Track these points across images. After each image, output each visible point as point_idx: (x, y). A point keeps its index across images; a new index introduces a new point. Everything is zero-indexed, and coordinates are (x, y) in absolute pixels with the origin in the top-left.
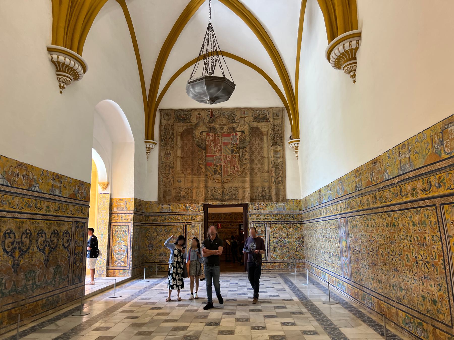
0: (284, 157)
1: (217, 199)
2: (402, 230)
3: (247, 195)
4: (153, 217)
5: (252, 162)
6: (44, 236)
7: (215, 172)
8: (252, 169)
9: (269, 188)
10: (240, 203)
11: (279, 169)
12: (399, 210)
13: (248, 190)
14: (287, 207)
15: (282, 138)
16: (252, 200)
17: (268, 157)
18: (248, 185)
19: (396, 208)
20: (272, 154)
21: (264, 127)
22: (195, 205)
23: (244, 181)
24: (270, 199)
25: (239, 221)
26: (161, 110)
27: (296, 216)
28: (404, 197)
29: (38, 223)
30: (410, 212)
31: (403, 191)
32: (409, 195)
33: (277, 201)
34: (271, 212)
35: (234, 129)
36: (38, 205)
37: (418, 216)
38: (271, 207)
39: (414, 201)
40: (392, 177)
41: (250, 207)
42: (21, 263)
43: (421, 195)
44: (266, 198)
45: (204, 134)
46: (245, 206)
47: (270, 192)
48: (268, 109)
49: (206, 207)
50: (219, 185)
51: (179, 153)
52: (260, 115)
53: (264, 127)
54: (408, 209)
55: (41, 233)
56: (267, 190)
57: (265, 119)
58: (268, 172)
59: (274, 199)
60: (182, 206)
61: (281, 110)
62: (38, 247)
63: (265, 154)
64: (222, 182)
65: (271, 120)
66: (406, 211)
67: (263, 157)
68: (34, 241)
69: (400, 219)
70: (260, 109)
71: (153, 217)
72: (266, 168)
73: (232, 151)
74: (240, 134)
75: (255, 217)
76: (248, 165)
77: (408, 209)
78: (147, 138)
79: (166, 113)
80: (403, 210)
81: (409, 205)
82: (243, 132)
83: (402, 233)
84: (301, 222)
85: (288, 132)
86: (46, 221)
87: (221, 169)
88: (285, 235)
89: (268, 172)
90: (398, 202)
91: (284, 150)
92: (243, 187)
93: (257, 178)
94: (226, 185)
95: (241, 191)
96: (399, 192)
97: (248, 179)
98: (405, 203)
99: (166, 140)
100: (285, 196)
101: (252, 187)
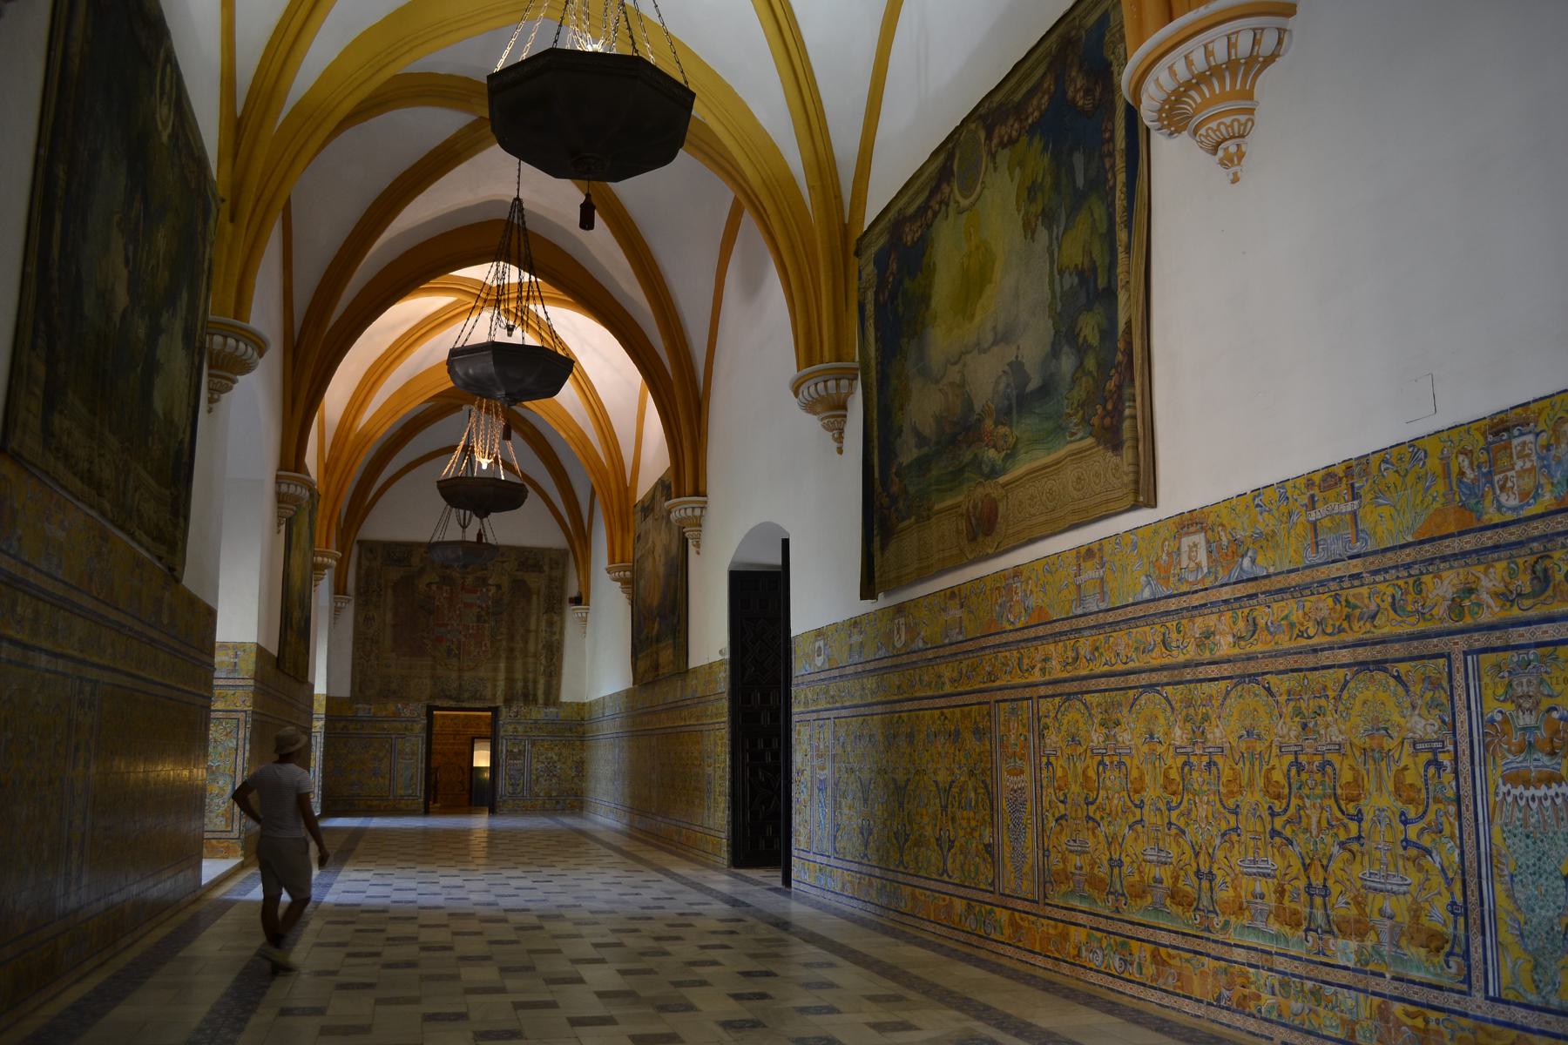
0: (562, 633)
1: (450, 698)
3: (500, 693)
4: (342, 724)
5: (511, 638)
7: (449, 651)
8: (511, 650)
9: (535, 682)
10: (487, 705)
11: (554, 652)
13: (501, 684)
14: (562, 715)
15: (561, 601)
16: (508, 701)
17: (537, 631)
18: (502, 676)
20: (543, 625)
21: (535, 581)
22: (412, 706)
23: (496, 669)
24: (535, 701)
25: (471, 731)
26: (361, 543)
27: (575, 727)
33: (546, 704)
34: (536, 721)
35: (483, 581)
38: (538, 713)
41: (504, 711)
44: (529, 698)
45: (434, 587)
46: (495, 711)
47: (535, 689)
48: (542, 551)
49: (430, 709)
50: (454, 675)
51: (389, 616)
52: (529, 559)
53: (535, 581)
56: (531, 685)
57: (537, 568)
58: (535, 656)
59: (541, 701)
60: (391, 707)
61: (563, 554)
63: (533, 627)
64: (460, 670)
65: (546, 568)
67: (528, 631)
70: (530, 550)
71: (342, 724)
72: (531, 648)
73: (479, 618)
74: (493, 589)
75: (510, 728)
76: (504, 643)
78: (337, 592)
79: (368, 547)
82: (499, 587)
84: (582, 738)
85: (573, 590)
87: (459, 648)
88: (555, 758)
89: (535, 656)
91: (562, 621)
92: (495, 680)
93: (518, 665)
94: (467, 675)
95: (489, 685)
97: (502, 665)
99: (367, 595)
100: (558, 696)
101: (510, 681)
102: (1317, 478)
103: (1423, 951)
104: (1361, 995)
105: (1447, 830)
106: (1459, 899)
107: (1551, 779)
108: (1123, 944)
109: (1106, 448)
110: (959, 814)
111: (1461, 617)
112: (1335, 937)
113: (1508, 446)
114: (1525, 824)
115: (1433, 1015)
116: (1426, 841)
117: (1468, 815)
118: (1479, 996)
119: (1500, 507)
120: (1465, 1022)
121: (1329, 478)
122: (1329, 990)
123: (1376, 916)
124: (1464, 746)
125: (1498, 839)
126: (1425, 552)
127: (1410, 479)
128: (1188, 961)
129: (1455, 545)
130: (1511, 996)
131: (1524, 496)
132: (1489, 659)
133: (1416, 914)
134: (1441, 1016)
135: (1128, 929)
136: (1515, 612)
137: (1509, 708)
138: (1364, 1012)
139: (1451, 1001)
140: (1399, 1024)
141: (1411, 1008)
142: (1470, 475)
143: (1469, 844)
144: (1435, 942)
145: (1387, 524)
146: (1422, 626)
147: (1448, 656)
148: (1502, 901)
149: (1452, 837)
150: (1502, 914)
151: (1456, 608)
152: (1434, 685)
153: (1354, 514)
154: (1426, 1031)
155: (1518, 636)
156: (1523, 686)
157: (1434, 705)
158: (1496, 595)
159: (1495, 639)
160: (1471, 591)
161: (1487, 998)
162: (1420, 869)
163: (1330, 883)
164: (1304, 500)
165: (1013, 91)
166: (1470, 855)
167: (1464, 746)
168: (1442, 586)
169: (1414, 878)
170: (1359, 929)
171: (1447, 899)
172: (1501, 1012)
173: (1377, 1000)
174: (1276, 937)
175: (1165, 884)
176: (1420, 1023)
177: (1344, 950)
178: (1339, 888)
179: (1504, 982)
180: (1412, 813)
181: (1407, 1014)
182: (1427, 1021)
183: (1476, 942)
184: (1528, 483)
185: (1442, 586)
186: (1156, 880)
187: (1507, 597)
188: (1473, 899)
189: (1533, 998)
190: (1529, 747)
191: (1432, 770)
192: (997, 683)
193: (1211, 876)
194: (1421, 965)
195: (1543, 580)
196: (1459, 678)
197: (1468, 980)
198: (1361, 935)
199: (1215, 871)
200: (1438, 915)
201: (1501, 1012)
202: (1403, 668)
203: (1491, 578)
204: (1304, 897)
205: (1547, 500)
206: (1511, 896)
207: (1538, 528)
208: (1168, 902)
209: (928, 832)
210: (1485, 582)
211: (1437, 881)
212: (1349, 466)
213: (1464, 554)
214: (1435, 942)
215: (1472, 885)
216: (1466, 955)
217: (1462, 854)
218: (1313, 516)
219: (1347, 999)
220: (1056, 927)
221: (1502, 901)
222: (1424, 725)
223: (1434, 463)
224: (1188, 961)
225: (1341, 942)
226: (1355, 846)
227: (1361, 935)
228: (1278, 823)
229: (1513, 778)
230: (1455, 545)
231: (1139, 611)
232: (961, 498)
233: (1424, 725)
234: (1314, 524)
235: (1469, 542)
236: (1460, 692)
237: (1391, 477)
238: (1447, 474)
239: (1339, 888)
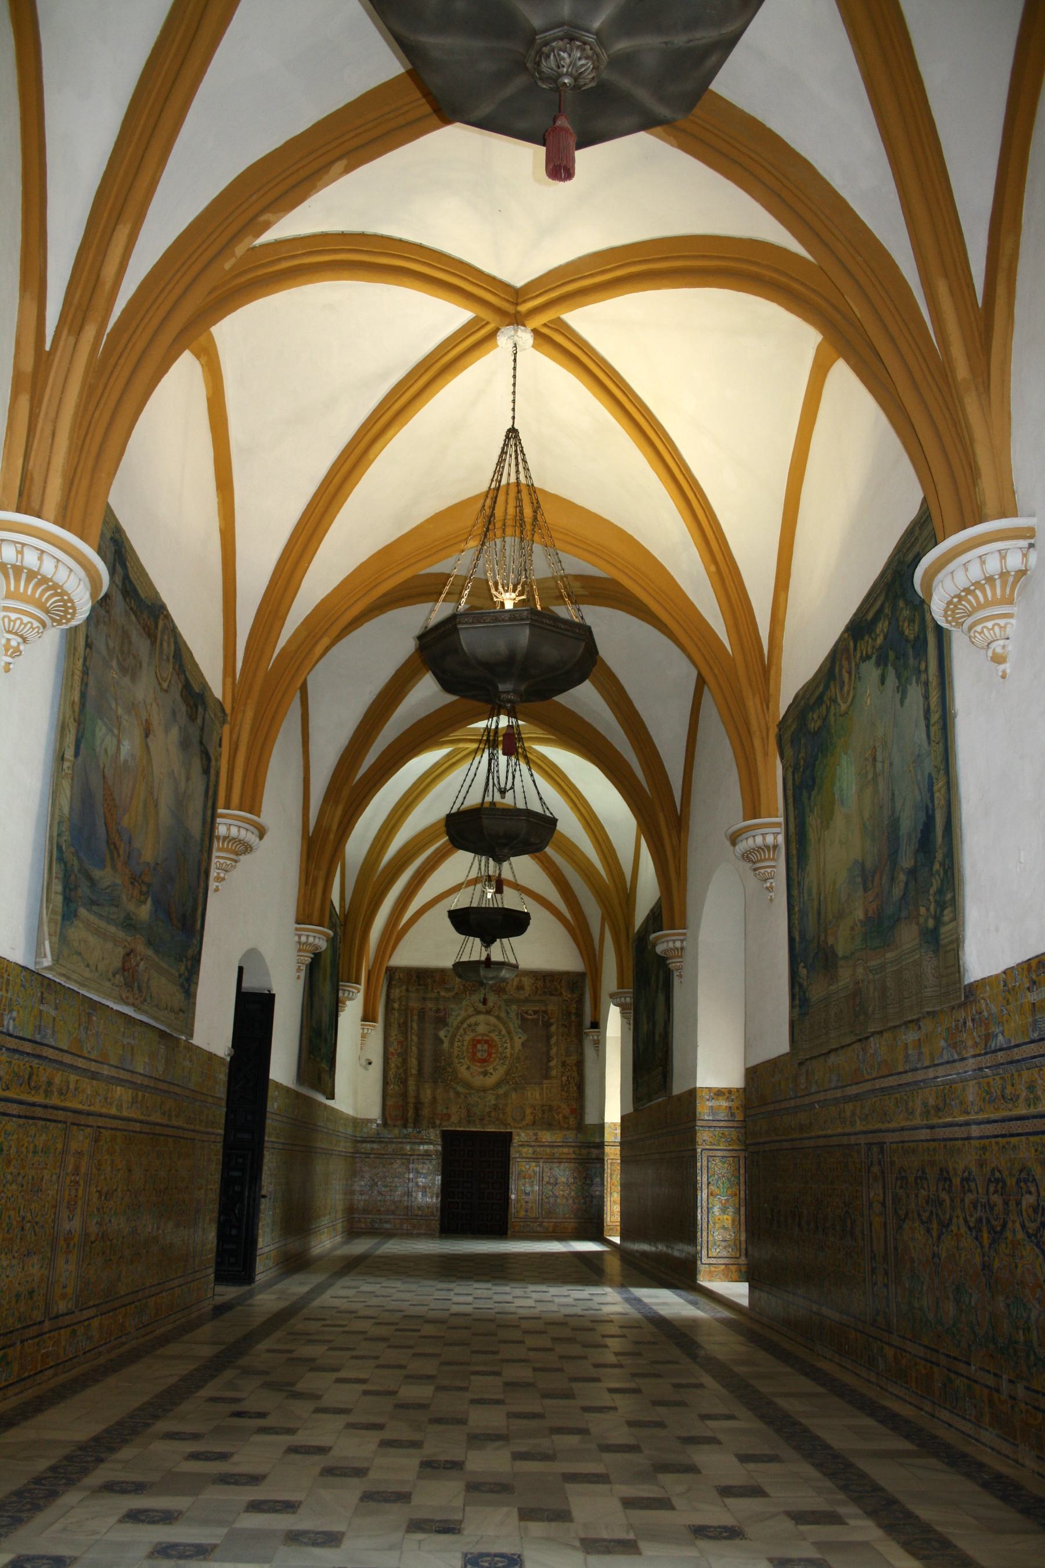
2: (13, 1163)
6: (1033, 1189)
12: (20, 1117)
19: (14, 1109)
28: (33, 1092)
29: (1015, 1148)
30: (36, 1125)
31: (34, 1077)
32: (41, 1091)
36: (1009, 1090)
37: (44, 1137)
39: (45, 1107)
40: (21, 1035)
42: (996, 1264)
43: (55, 1100)
54: (33, 1118)
55: (1026, 1181)
62: (1023, 1226)
66: (31, 1122)
68: (1012, 1204)
69: (15, 1136)
77: (33, 1118)
80: (26, 1117)
81: (39, 1112)
83: (11, 1169)
86: (1031, 1138)
90: (24, 1097)
96: (27, 1077)
98: (34, 1105)
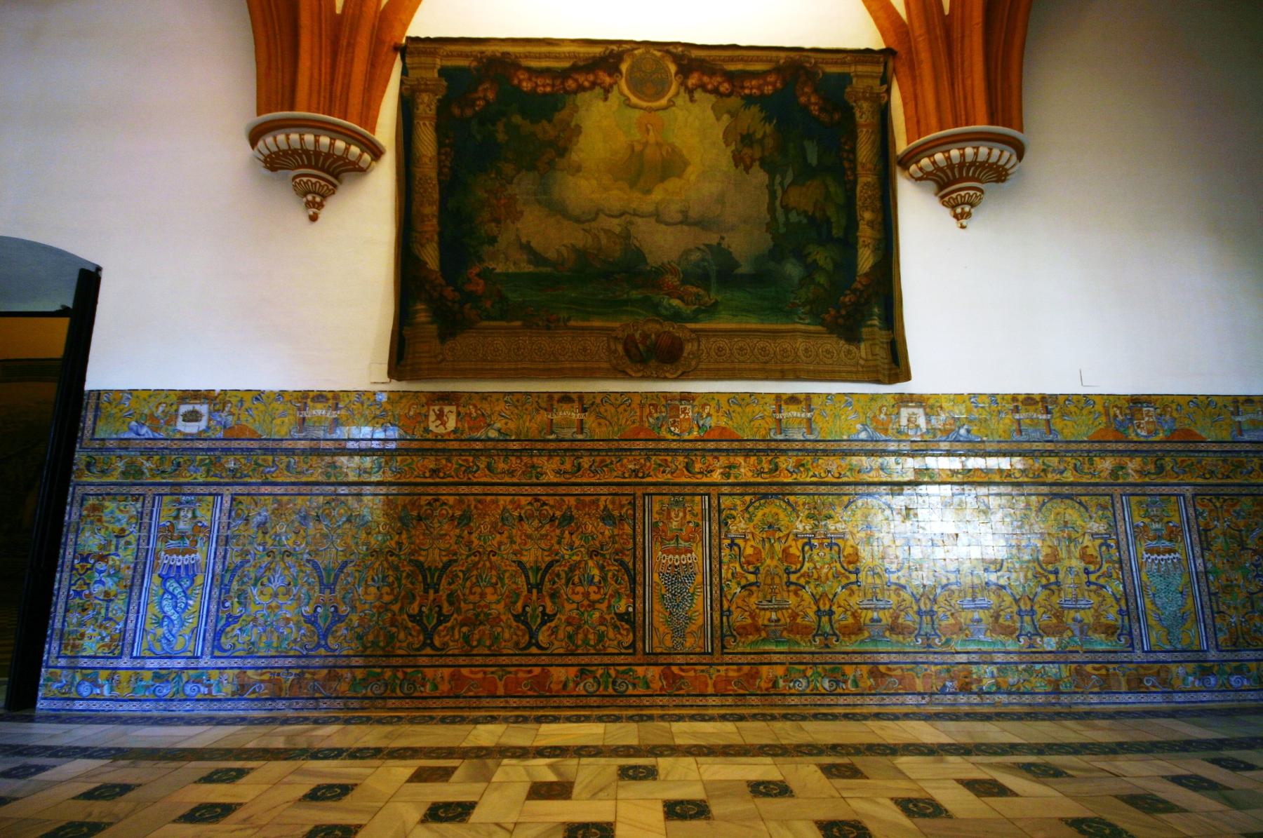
102: (1020, 398)
103: (1103, 636)
104: (1062, 666)
105: (1115, 575)
106: (1124, 608)
107: (1170, 551)
108: (833, 670)
109: (840, 337)
110: (565, 591)
111: (1117, 478)
112: (1042, 637)
113: (1141, 410)
114: (1158, 570)
115: (1110, 666)
116: (1102, 581)
117: (1126, 568)
118: (1139, 652)
119: (1137, 435)
120: (1131, 666)
121: (1029, 400)
122: (1038, 667)
123: (1070, 621)
124: (1122, 537)
125: (1144, 578)
126: (1096, 447)
127: (1085, 412)
128: (911, 669)
129: (1114, 446)
130: (1157, 648)
131: (1149, 432)
132: (1134, 499)
133: (1097, 616)
134: (1116, 666)
135: (840, 658)
136: (1147, 480)
137: (1147, 520)
138: (1065, 673)
139: (1122, 657)
140: (1089, 675)
141: (1097, 666)
142: (1120, 418)
143: (1128, 582)
144: (1110, 630)
145: (1074, 429)
146: (1093, 481)
147: (1111, 496)
148: (1149, 605)
149: (1118, 579)
150: (1149, 612)
151: (1114, 473)
152: (1104, 508)
153: (1048, 421)
154: (1108, 675)
155: (1149, 490)
156: (1154, 511)
157: (1104, 517)
158: (1136, 471)
159: (1137, 490)
160: (1122, 468)
161: (1144, 651)
162: (1099, 595)
163: (1036, 608)
164: (1011, 406)
165: (732, 60)
166: (1129, 587)
167: (1122, 537)
168: (1106, 464)
169: (1095, 599)
170: (1057, 630)
171: (1116, 608)
172: (1153, 657)
173: (1073, 666)
174: (994, 643)
175: (884, 622)
176: (1103, 672)
177: (1051, 643)
178: (1042, 610)
179: (1153, 641)
180: (1092, 568)
181: (1095, 669)
182: (1108, 670)
183: (1135, 626)
184: (1151, 427)
185: (1106, 464)
186: (872, 620)
187: (1141, 472)
188: (1132, 607)
189: (1168, 647)
190: (1159, 538)
191: (1104, 548)
192: (648, 480)
193: (932, 613)
194: (1100, 642)
195: (1161, 469)
196: (1118, 506)
197: (1132, 645)
198: (1060, 633)
199: (834, 608)
200: (1111, 616)
201: (1153, 657)
202: (1083, 499)
203: (1133, 465)
204: (1016, 617)
205: (1161, 436)
206: (1153, 603)
207: (1158, 447)
208: (887, 634)
209: (498, 609)
210: (1130, 465)
211: (1110, 600)
212: (1044, 398)
213: (1119, 451)
214: (1110, 630)
215: (1131, 600)
216: (1130, 634)
217: (1124, 587)
218: (1017, 416)
219: (1052, 670)
220: (739, 670)
221: (1149, 605)
222: (1098, 527)
223: (1099, 407)
224: (911, 669)
225: (1046, 639)
226: (1054, 587)
227: (1060, 633)
228: (1093, 578)
229: (1150, 551)
230: (1114, 446)
231: (835, 446)
232: (617, 324)
233: (1098, 527)
234: (1019, 421)
235: (1121, 447)
236: (1118, 512)
237: (1072, 408)
238: (1107, 414)
239: (1042, 610)
